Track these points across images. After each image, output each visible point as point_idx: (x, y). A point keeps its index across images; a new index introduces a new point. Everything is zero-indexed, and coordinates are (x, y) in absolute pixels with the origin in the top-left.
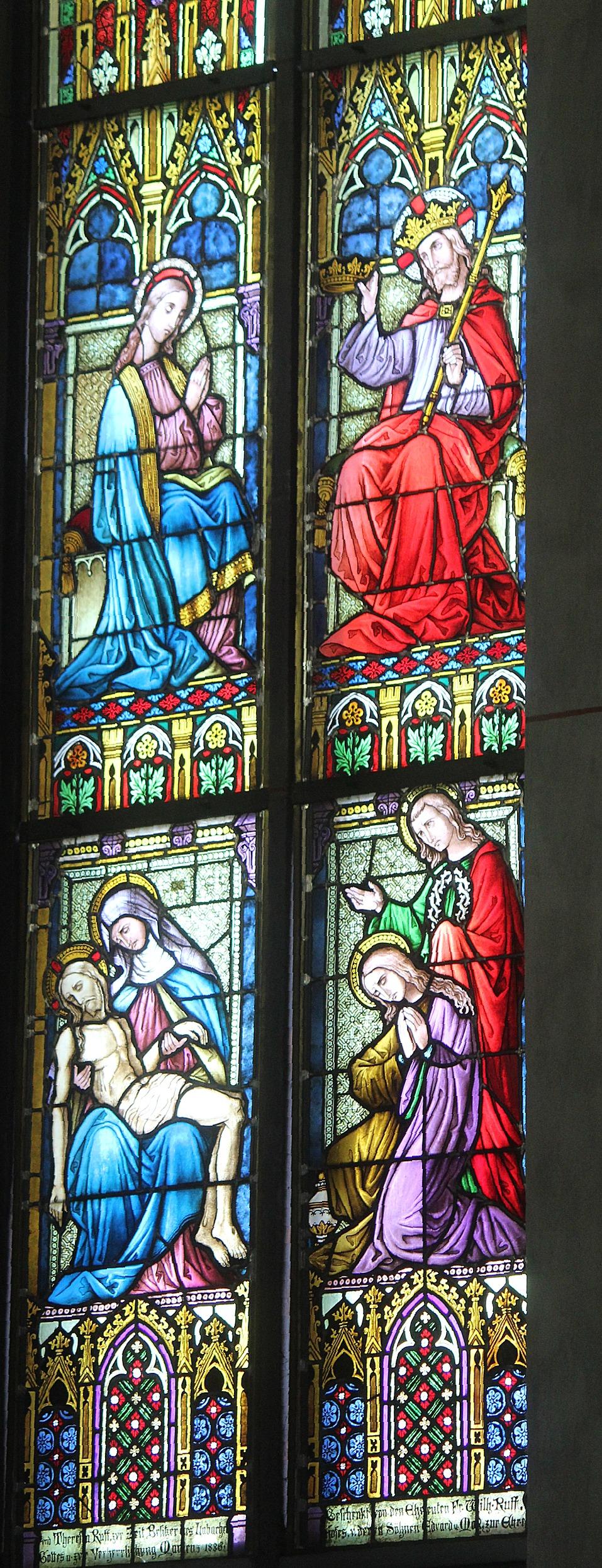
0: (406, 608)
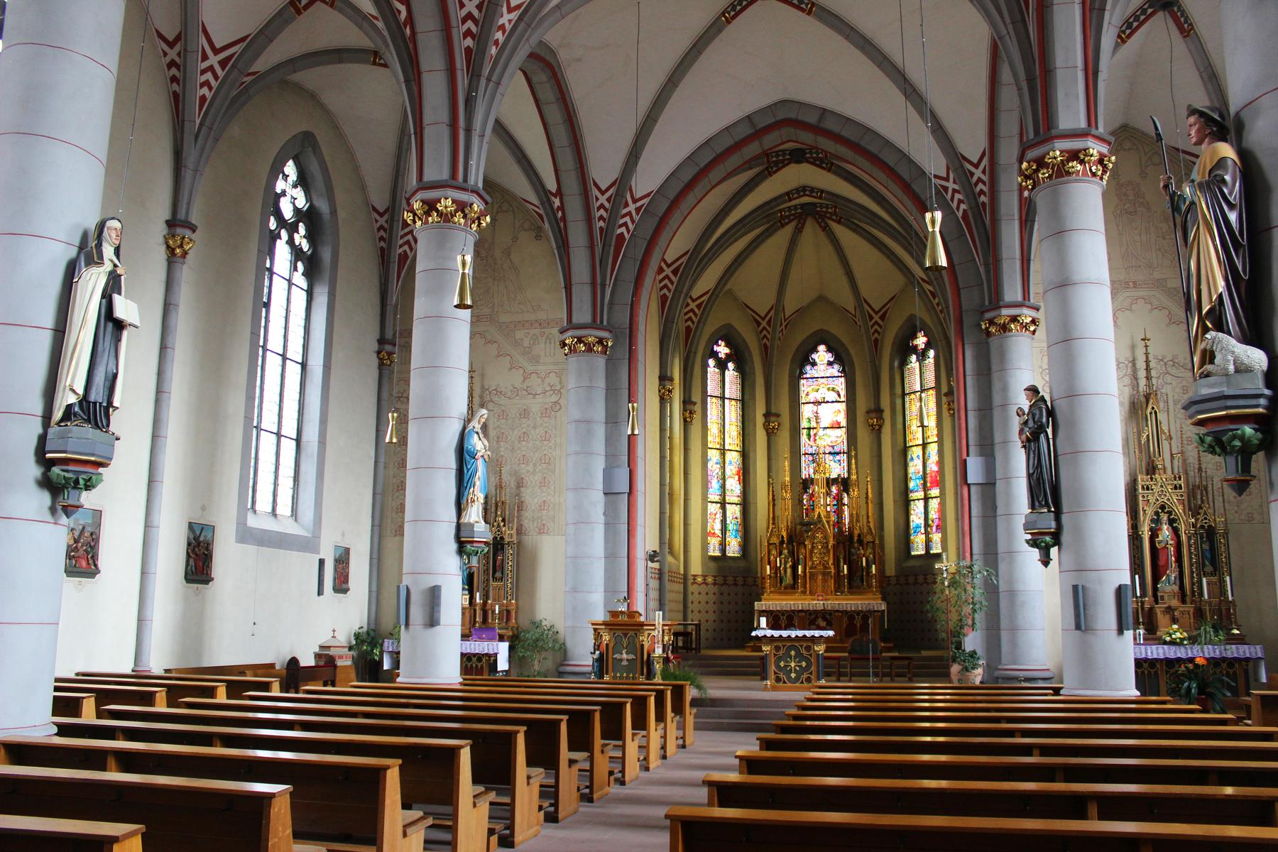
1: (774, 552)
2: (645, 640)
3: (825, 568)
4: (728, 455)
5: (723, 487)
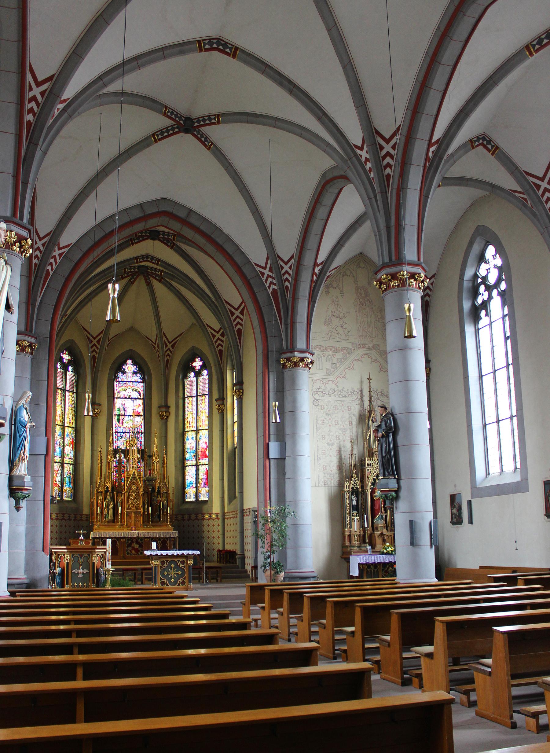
1: (100, 498)
2: (96, 559)
3: (137, 509)
5: (63, 452)
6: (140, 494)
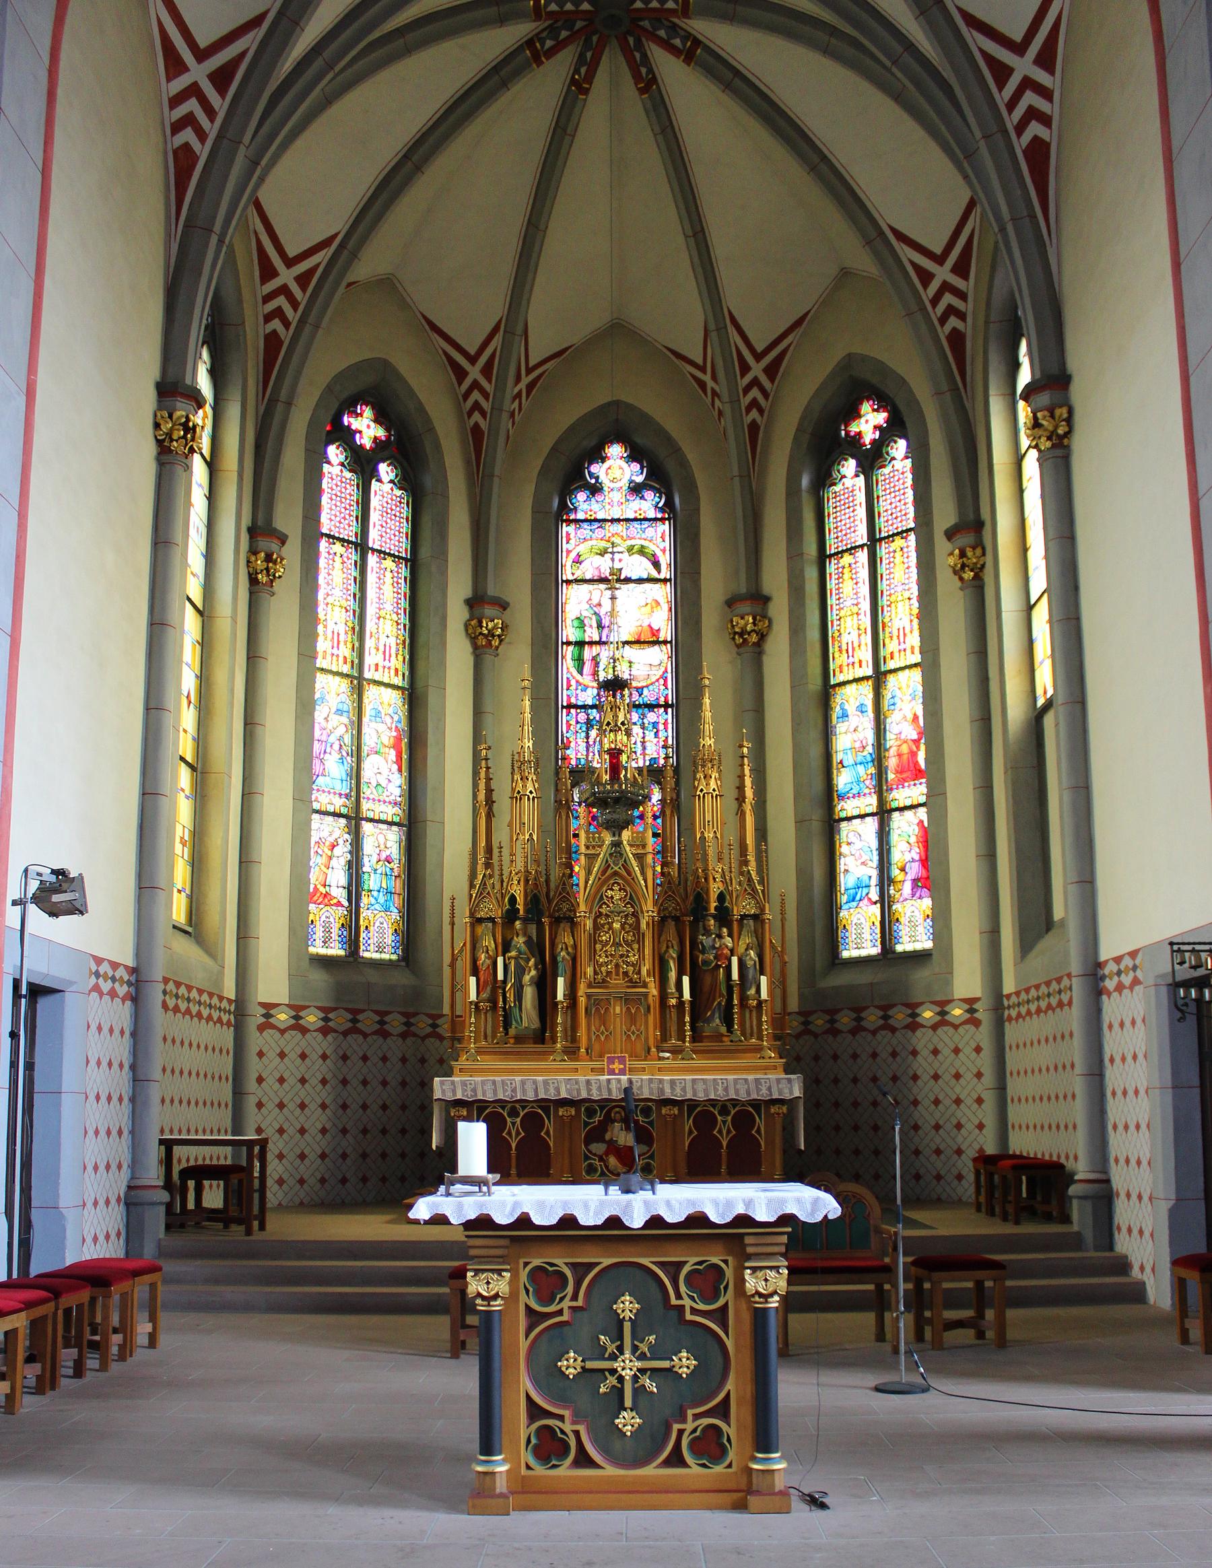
0: (904, 776)
1: (488, 942)
4: (372, 695)
5: (356, 775)
6: (643, 926)
